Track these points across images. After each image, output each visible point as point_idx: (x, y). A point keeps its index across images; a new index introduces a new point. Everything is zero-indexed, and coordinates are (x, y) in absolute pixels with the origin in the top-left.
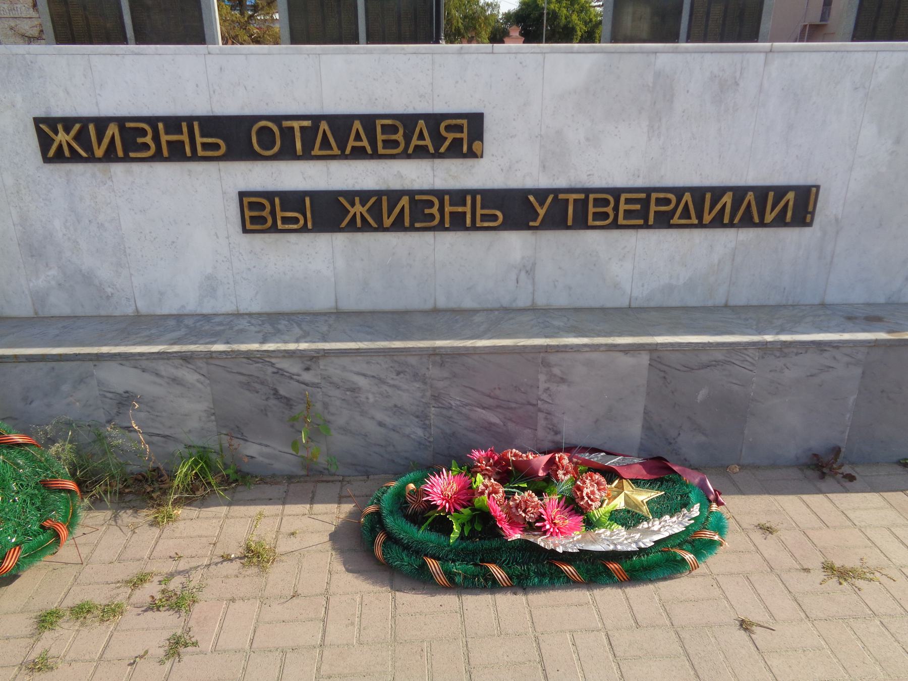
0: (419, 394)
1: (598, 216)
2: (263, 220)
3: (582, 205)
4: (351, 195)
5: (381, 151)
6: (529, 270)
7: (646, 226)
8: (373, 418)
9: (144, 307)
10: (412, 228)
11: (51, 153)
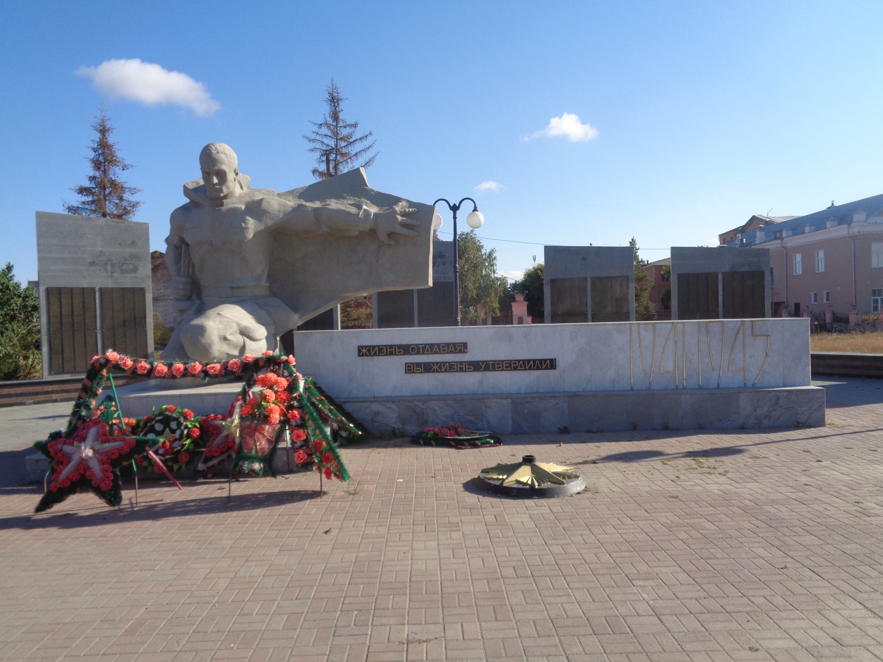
1: (498, 367)
2: (411, 370)
3: (493, 365)
4: (433, 363)
6: (481, 382)
7: (511, 370)
9: (377, 395)
10: (449, 372)
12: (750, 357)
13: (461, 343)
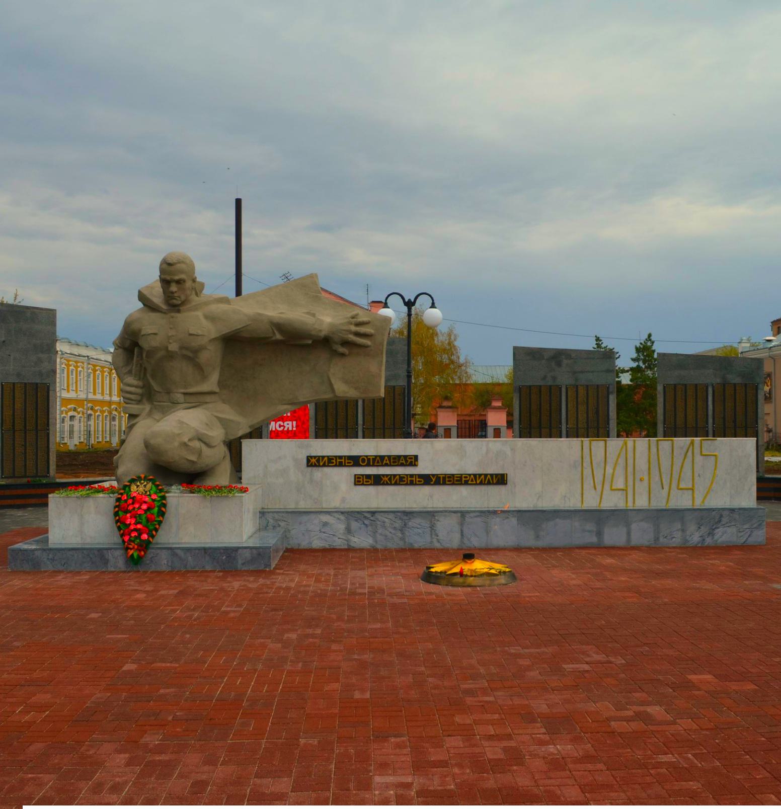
0: (401, 524)
1: (449, 481)
2: (359, 481)
4: (383, 475)
5: (392, 464)
7: (461, 484)
8: (388, 531)
11: (309, 464)
12: (699, 476)
13: (413, 456)
